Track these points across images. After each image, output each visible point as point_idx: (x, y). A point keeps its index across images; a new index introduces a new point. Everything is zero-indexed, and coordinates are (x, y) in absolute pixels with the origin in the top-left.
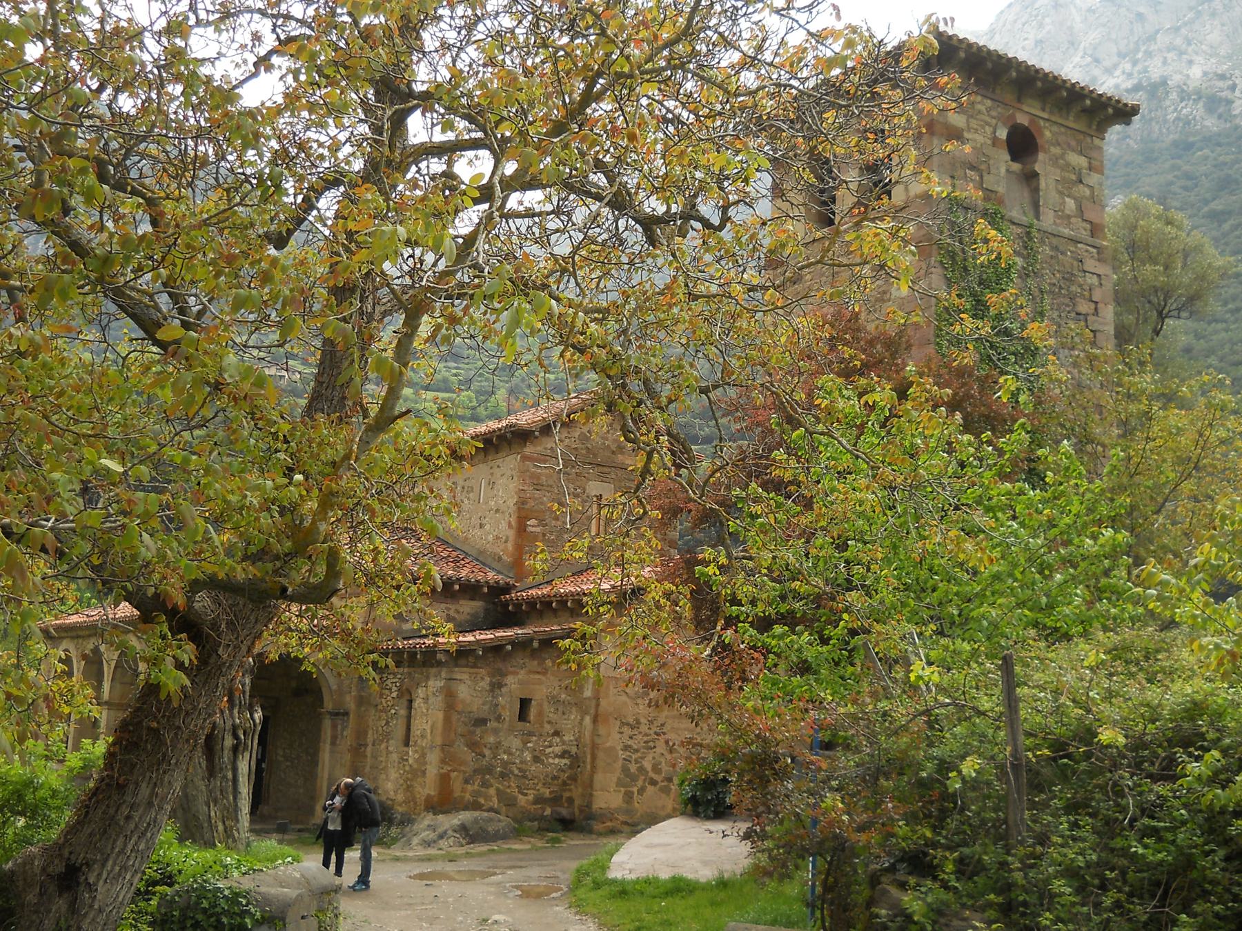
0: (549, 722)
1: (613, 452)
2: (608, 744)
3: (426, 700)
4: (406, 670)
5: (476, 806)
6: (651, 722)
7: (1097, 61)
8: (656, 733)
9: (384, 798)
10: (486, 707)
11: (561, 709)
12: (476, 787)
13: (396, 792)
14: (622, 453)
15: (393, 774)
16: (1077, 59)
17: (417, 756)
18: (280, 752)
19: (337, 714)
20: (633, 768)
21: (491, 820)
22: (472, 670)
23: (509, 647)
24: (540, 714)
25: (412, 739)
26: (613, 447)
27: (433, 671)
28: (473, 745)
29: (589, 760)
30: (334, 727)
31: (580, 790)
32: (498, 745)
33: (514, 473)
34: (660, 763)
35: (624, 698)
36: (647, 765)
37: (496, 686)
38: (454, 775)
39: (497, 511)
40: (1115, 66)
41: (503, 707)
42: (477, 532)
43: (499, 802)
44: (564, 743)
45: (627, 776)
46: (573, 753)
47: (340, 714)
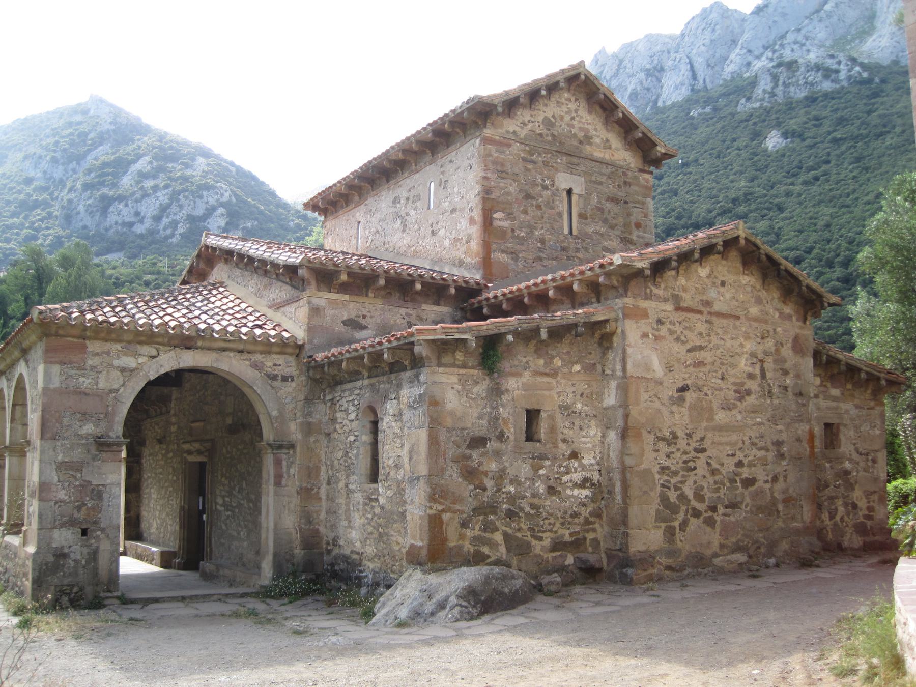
0: (564, 441)
1: (581, 142)
2: (643, 467)
3: (399, 416)
4: (366, 382)
5: (477, 559)
6: (689, 435)
7: (750, 51)
8: (697, 450)
9: (347, 552)
10: (483, 422)
11: (577, 422)
12: (477, 532)
13: (364, 542)
14: (590, 144)
15: (358, 520)
16: (737, 51)
17: (390, 493)
18: (220, 501)
19: (280, 447)
20: (673, 496)
21: (504, 578)
22: (462, 371)
23: (510, 338)
24: (552, 429)
25: (381, 471)
26: (581, 135)
27: (408, 374)
28: (471, 474)
29: (618, 487)
30: (278, 463)
31: (606, 528)
32: (501, 476)
33: (473, 162)
34: (702, 488)
35: (657, 404)
36: (689, 491)
37: (496, 391)
38: (446, 517)
39: (453, 211)
40: (762, 54)
41: (506, 422)
42: (429, 241)
43: (509, 550)
44: (584, 468)
45: (666, 507)
46: (596, 482)
47: (283, 446)
